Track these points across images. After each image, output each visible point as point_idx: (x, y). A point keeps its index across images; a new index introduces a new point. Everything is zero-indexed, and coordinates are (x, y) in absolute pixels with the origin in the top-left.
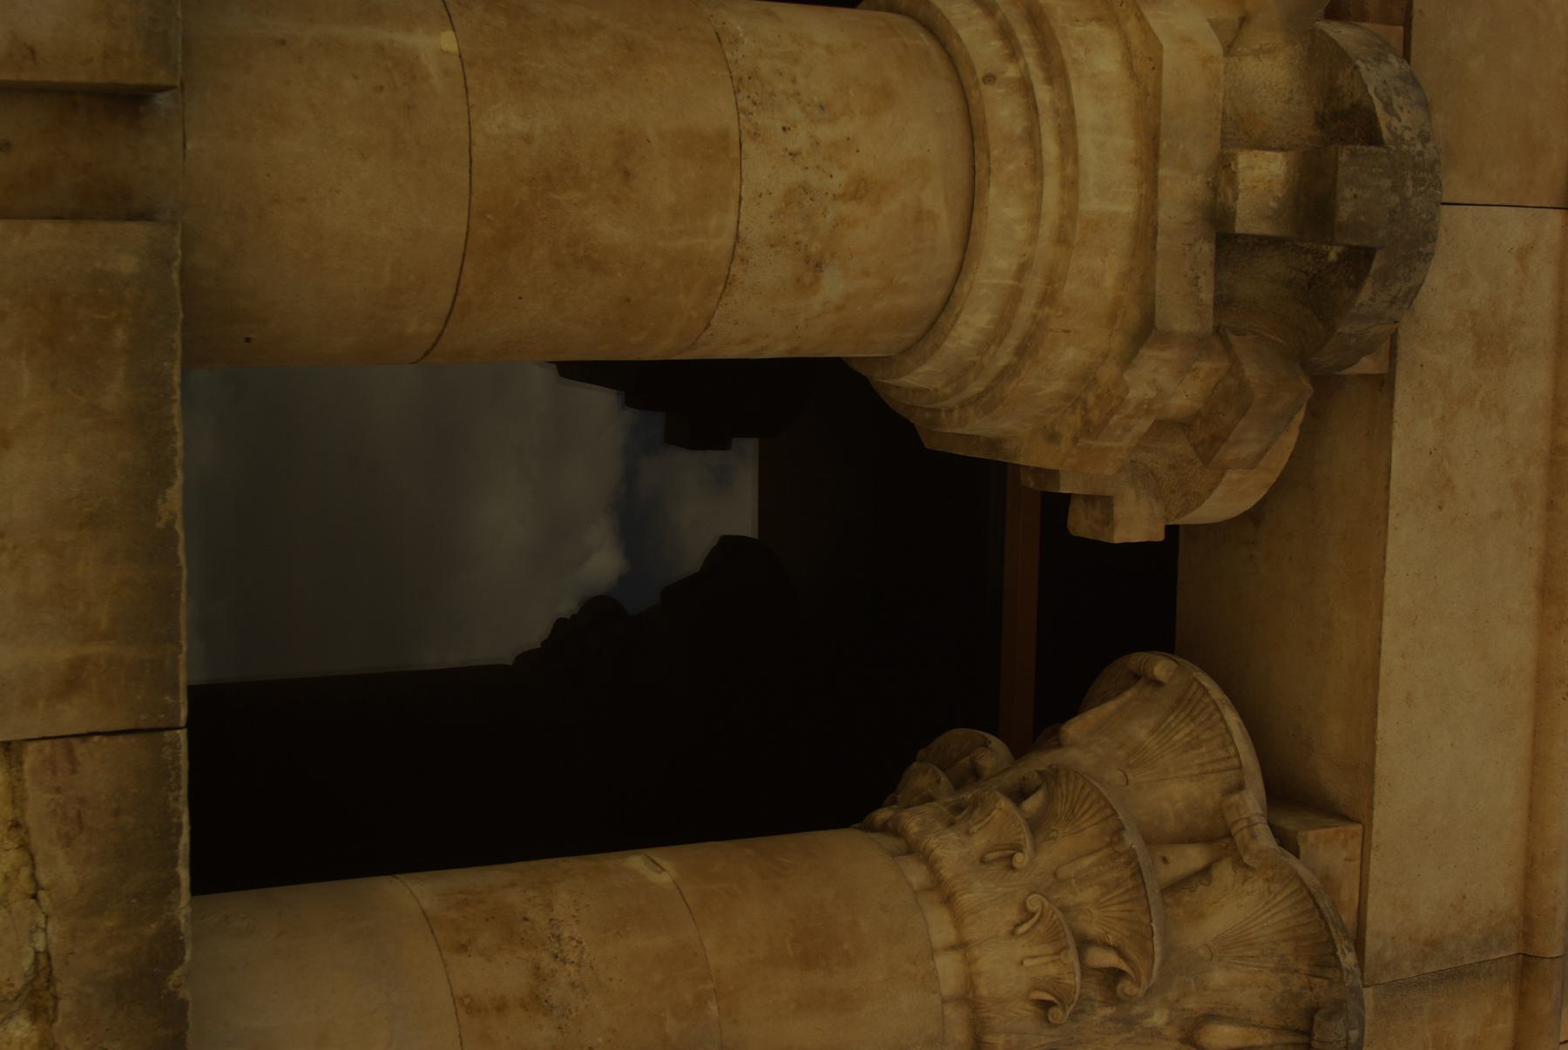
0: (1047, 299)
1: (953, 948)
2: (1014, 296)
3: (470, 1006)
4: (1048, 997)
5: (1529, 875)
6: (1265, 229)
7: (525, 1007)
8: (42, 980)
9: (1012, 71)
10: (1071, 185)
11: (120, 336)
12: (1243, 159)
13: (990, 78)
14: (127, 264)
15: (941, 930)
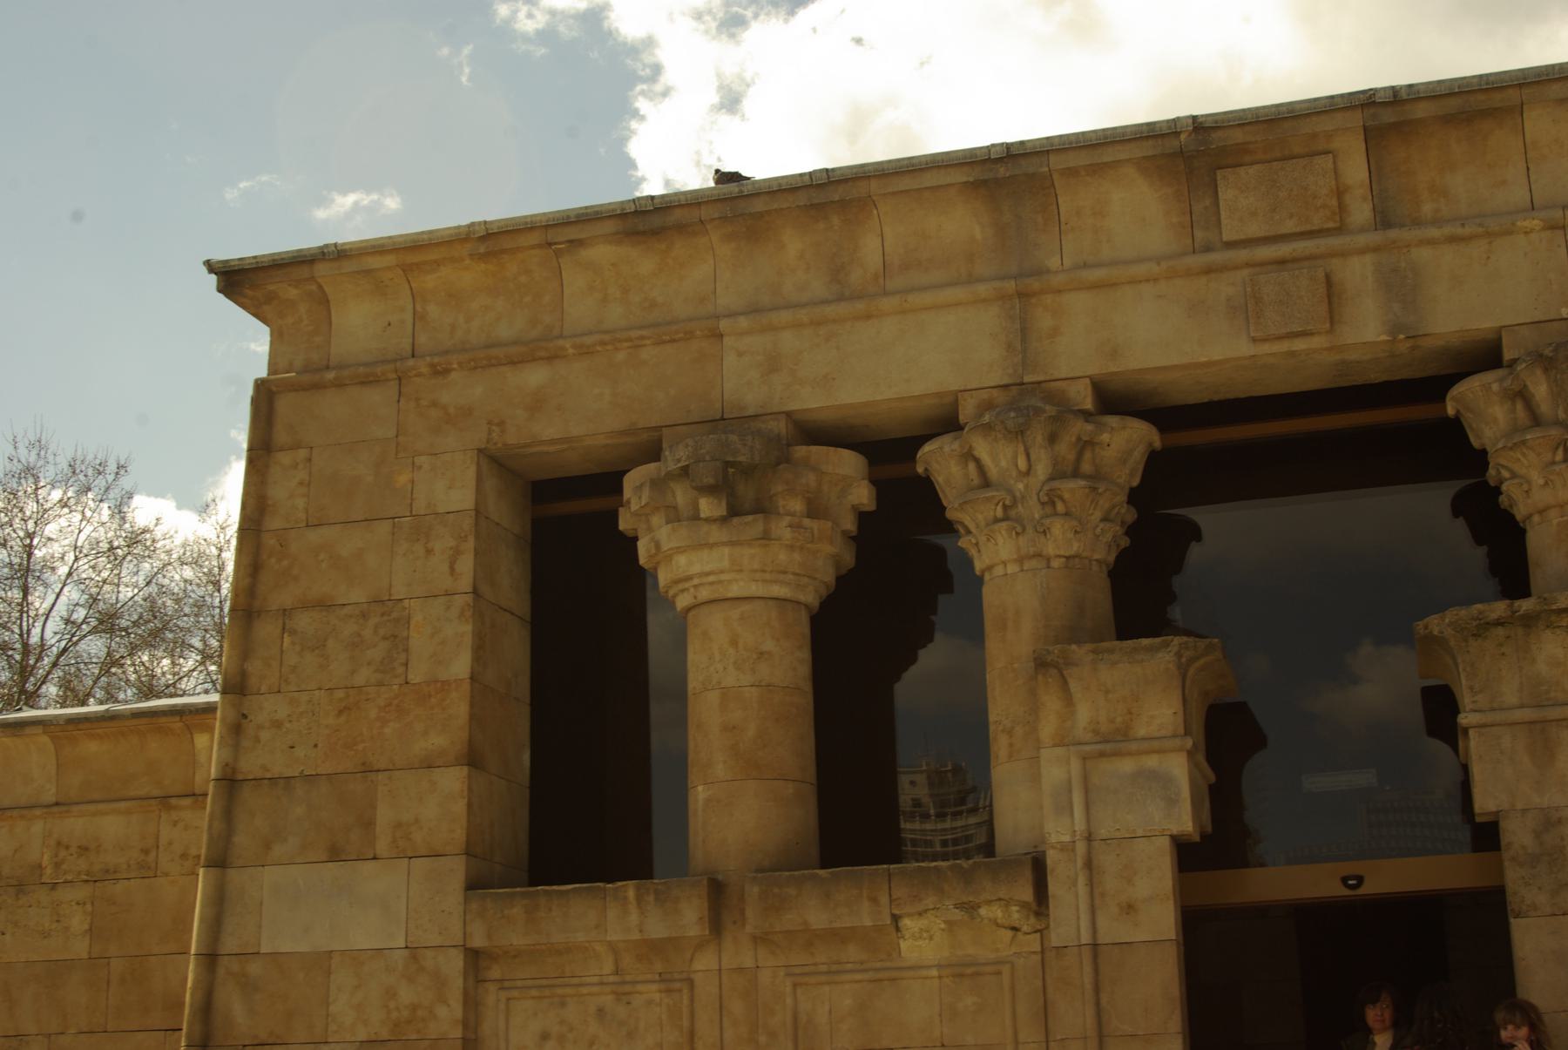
0: (764, 571)
1: (1005, 566)
2: (765, 581)
3: (1010, 756)
4: (1014, 533)
5: (984, 301)
6: (724, 504)
7: (1011, 737)
8: (965, 906)
9: (692, 590)
10: (722, 572)
11: (776, 890)
12: (702, 515)
13: (695, 597)
14: (756, 889)
15: (999, 571)
